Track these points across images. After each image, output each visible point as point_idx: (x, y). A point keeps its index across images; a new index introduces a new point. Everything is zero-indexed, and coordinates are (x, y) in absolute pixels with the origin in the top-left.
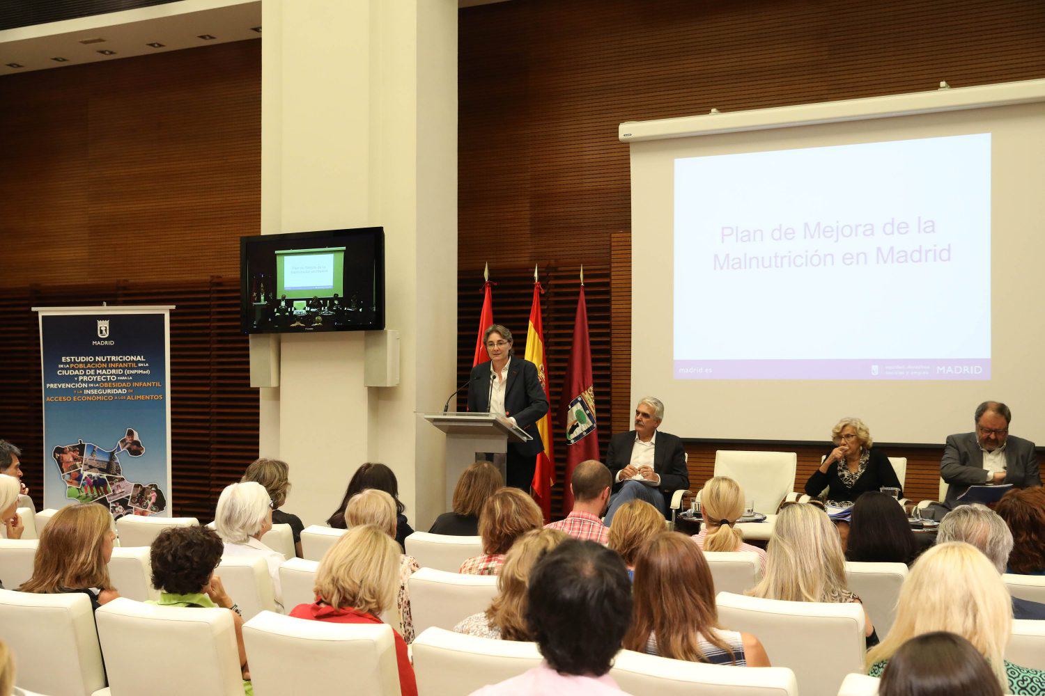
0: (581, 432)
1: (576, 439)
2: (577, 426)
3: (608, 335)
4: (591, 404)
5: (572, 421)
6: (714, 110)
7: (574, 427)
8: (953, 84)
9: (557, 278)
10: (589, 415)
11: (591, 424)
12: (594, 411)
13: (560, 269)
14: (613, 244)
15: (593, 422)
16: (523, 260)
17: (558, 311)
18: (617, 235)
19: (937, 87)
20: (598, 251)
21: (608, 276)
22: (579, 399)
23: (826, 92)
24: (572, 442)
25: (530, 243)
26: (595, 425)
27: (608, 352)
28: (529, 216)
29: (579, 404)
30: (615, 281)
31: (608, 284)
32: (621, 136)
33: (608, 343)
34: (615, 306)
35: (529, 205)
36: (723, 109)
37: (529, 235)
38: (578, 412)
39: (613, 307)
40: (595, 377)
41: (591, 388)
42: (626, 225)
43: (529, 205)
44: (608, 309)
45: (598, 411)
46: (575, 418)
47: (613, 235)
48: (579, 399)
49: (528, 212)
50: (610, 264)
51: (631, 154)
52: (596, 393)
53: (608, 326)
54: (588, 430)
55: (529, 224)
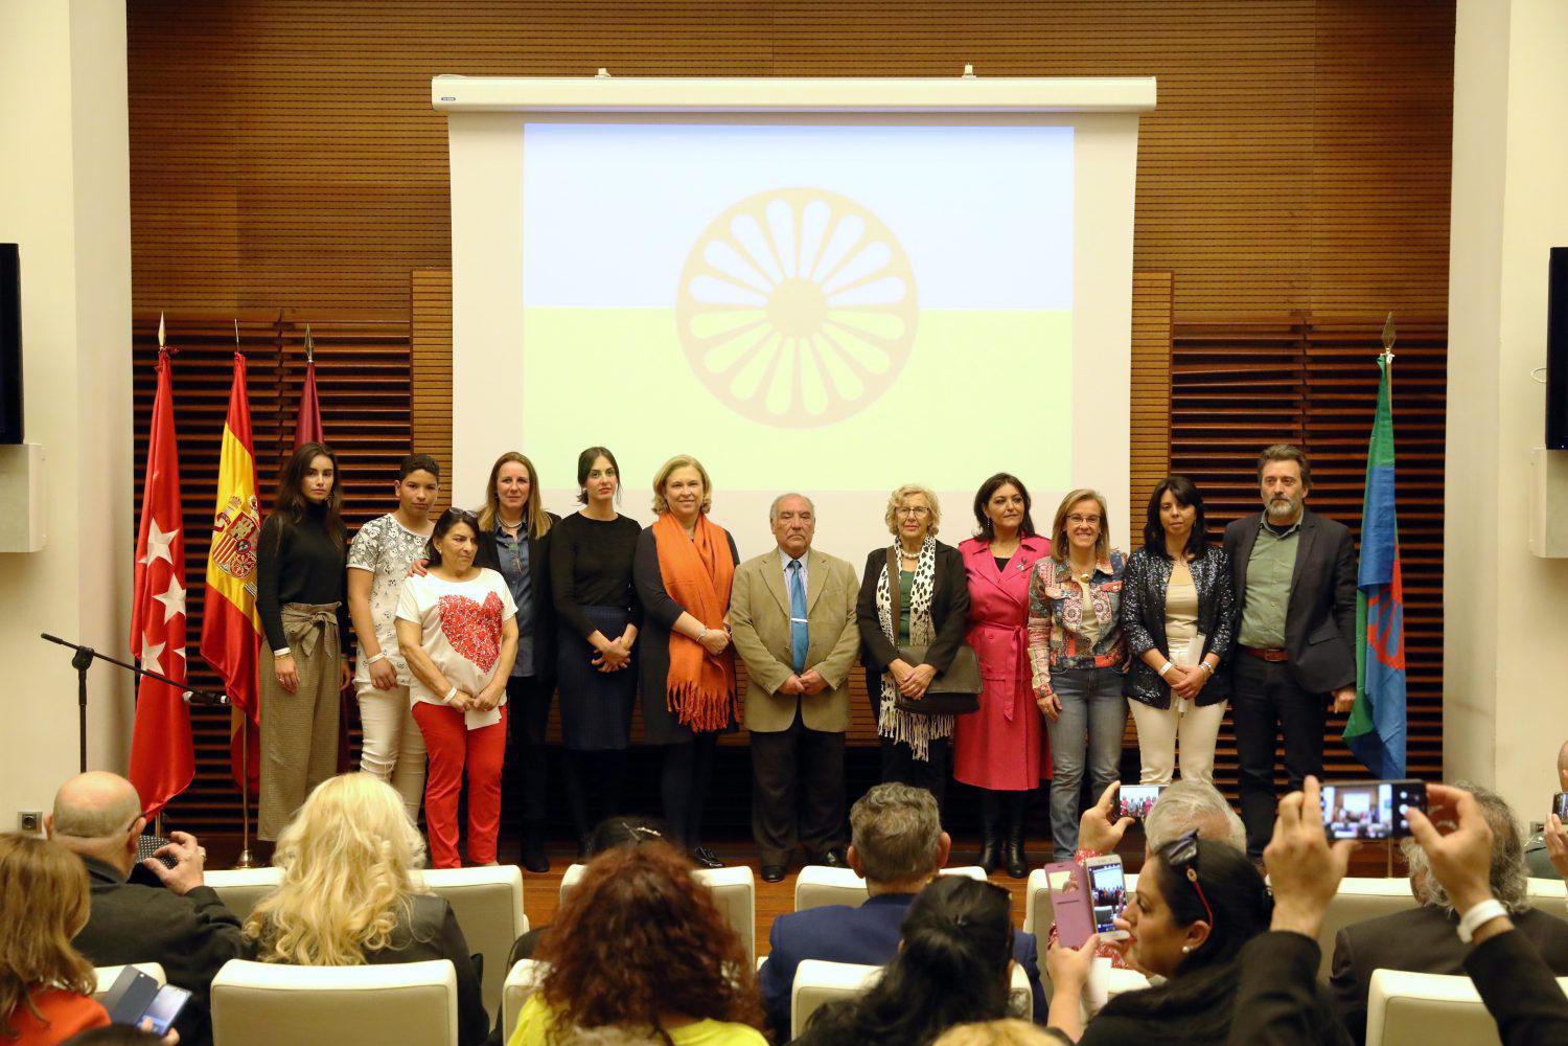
8: (978, 73)
18: (426, 274)
19: (959, 73)
20: (373, 297)
21: (406, 342)
23: (770, 57)
28: (235, 225)
30: (421, 354)
31: (406, 357)
32: (436, 99)
34: (421, 399)
37: (236, 261)
39: (416, 399)
42: (440, 255)
43: (235, 205)
44: (406, 402)
49: (235, 218)
50: (411, 323)
51: (451, 136)
55: (236, 240)
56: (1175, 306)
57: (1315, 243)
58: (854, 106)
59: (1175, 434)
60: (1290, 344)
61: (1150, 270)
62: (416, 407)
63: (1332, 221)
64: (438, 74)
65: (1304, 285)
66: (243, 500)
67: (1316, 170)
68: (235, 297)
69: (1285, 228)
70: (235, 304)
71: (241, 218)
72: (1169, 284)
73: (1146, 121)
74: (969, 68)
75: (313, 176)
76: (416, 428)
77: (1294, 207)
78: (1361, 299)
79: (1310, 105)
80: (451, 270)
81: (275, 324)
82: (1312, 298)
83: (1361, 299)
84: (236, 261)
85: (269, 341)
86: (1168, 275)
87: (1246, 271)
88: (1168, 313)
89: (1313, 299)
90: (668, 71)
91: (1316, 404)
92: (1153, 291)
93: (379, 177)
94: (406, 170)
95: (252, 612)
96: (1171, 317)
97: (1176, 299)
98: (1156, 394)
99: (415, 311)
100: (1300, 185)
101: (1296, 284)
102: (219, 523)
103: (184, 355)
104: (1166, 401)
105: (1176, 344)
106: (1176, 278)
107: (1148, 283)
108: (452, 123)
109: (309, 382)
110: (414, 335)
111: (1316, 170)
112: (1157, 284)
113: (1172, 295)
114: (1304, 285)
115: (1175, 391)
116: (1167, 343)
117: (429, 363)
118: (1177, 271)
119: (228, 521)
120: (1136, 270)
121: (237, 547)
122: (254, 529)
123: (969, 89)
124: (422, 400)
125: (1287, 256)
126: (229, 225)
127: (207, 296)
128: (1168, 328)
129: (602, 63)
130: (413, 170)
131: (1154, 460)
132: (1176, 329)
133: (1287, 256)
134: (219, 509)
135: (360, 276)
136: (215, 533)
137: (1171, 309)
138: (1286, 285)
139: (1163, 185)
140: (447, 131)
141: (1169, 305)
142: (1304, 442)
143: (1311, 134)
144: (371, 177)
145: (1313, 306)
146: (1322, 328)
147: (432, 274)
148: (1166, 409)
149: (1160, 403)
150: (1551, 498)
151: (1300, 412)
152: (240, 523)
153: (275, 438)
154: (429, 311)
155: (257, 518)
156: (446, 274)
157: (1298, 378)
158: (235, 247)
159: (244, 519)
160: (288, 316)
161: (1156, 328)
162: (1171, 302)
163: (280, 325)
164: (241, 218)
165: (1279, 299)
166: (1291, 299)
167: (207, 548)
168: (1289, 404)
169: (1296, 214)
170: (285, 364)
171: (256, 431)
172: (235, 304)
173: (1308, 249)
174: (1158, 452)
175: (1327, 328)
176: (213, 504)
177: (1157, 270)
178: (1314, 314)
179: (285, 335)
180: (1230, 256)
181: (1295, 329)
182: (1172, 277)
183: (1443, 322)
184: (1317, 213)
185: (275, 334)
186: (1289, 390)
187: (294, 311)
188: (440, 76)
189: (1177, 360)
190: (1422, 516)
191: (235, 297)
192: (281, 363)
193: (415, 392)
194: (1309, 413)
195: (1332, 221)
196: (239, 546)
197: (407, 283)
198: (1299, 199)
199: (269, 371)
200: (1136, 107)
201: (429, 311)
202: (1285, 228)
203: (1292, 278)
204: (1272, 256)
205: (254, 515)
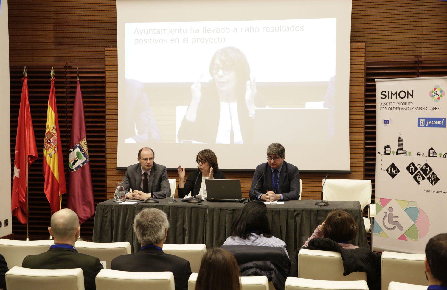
0: (80, 164)
1: (76, 168)
2: (77, 160)
4: (85, 148)
5: (74, 158)
7: (75, 162)
10: (84, 154)
11: (85, 159)
12: (87, 152)
15: (87, 158)
16: (49, 60)
22: (78, 145)
24: (75, 170)
26: (88, 160)
35: (52, 27)
37: (53, 46)
38: (78, 154)
40: (87, 132)
41: (85, 139)
43: (52, 27)
45: (89, 151)
46: (76, 156)
48: (78, 145)
49: (53, 32)
52: (88, 141)
54: (83, 163)
56: (367, 55)
60: (414, 68)
65: (419, 46)
68: (53, 58)
69: (412, 26)
70: (53, 60)
71: (55, 32)
75: (78, 17)
82: (423, 51)
84: (53, 46)
85: (63, 72)
86: (364, 44)
88: (364, 58)
92: (359, 50)
94: (107, 14)
96: (365, 59)
97: (367, 53)
98: (360, 87)
101: (417, 46)
105: (367, 69)
107: (356, 47)
110: (106, 70)
111: (425, 4)
112: (360, 47)
113: (365, 51)
114: (419, 46)
115: (367, 86)
116: (364, 68)
118: (367, 43)
120: (351, 42)
124: (109, 91)
128: (364, 63)
132: (367, 63)
135: (93, 50)
137: (365, 57)
139: (367, 12)
141: (364, 55)
144: (96, 17)
145: (423, 54)
147: (111, 49)
148: (363, 92)
153: (64, 105)
158: (53, 41)
160: (69, 64)
161: (360, 63)
162: (365, 54)
163: (66, 67)
164: (55, 32)
165: (410, 52)
166: (416, 52)
169: (417, 20)
170: (68, 80)
172: (53, 60)
173: (421, 33)
174: (360, 108)
178: (423, 57)
179: (68, 70)
180: (392, 37)
181: (416, 62)
182: (365, 46)
185: (64, 70)
191: (53, 58)
198: (418, 15)
199: (63, 82)
201: (111, 62)
202: (412, 26)
203: (415, 44)
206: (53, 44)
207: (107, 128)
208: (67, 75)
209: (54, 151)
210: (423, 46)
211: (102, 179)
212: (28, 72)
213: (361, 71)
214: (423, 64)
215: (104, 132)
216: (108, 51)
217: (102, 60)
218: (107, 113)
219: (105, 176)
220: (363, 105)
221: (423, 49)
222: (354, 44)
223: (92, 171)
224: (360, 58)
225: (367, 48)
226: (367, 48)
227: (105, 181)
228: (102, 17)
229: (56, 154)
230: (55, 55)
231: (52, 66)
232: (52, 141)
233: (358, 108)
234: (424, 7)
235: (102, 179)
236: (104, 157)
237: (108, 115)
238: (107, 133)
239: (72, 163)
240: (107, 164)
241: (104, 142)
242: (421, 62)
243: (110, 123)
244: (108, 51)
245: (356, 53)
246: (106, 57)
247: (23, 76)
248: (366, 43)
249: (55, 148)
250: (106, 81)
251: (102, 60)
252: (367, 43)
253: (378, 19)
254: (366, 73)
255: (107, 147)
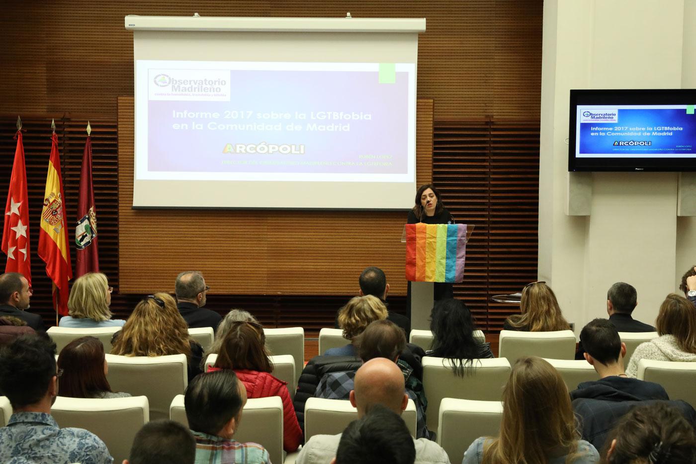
3: (116, 170)
6: (196, 14)
8: (353, 16)
9: (70, 126)
13: (73, 120)
14: (119, 104)
16: (41, 111)
17: (71, 151)
18: (123, 98)
19: (345, 16)
21: (116, 127)
25: (47, 98)
27: (116, 183)
28: (45, 77)
29: (86, 220)
30: (122, 131)
31: (115, 133)
32: (127, 25)
33: (116, 176)
36: (202, 14)
39: (119, 150)
44: (116, 152)
47: (119, 98)
49: (45, 74)
53: (116, 164)
57: (495, 87)
58: (263, 29)
59: (435, 167)
60: (485, 130)
61: (424, 98)
62: (119, 154)
63: (502, 78)
64: (127, 15)
66: (56, 194)
67: (496, 57)
69: (483, 81)
72: (432, 104)
73: (421, 36)
74: (349, 14)
75: (78, 57)
76: (120, 162)
77: (487, 72)
78: (514, 111)
79: (493, 30)
80: (134, 97)
81: (62, 119)
83: (514, 111)
84: (45, 93)
86: (432, 101)
87: (467, 99)
88: (432, 116)
89: (494, 111)
90: (232, 14)
91: (495, 154)
92: (426, 107)
93: (107, 57)
95: (57, 239)
97: (435, 111)
99: (119, 114)
100: (489, 63)
101: (487, 105)
102: (45, 203)
103: (28, 132)
104: (431, 153)
105: (435, 129)
106: (435, 102)
107: (423, 104)
108: (135, 36)
109: (88, 143)
111: (496, 57)
113: (433, 108)
114: (491, 105)
115: (435, 149)
116: (431, 128)
117: (125, 135)
118: (436, 99)
119: (49, 202)
120: (418, 98)
121: (52, 213)
122: (59, 206)
123: (349, 23)
125: (484, 93)
126: (43, 77)
127: (35, 107)
128: (432, 122)
129: (195, 11)
130: (120, 55)
131: (426, 177)
132: (435, 123)
133: (484, 93)
134: (46, 197)
136: (44, 207)
137: (433, 115)
138: (484, 105)
140: (133, 38)
141: (432, 113)
142: (490, 170)
143: (494, 42)
144: (102, 57)
145: (494, 114)
146: (499, 123)
147: (126, 98)
148: (431, 156)
149: (429, 154)
150: (571, 191)
151: (488, 158)
152: (54, 203)
154: (125, 114)
155: (61, 202)
156: (131, 98)
157: (487, 144)
159: (56, 202)
160: (67, 115)
161: (427, 122)
167: (40, 212)
168: (484, 155)
169: (488, 75)
171: (61, 163)
172: (45, 110)
173: (493, 90)
175: (502, 123)
176: (43, 194)
177: (429, 98)
178: (494, 117)
180: (460, 93)
181: (487, 123)
183: (538, 121)
184: (496, 75)
185: (62, 123)
186: (484, 148)
187: (70, 114)
188: (129, 16)
189: (435, 136)
190: (530, 201)
192: (64, 135)
193: (119, 147)
194: (492, 158)
195: (502, 78)
196: (54, 212)
197: (115, 102)
200: (418, 30)
201: (125, 114)
203: (486, 102)
204: (478, 93)
205: (60, 200)
206: (46, 89)
207: (120, 196)
208: (65, 130)
209: (61, 225)
210: (495, 105)
211: (114, 259)
212: (24, 125)
213: (429, 132)
214: (495, 125)
215: (117, 201)
216: (121, 101)
217: (114, 111)
218: (120, 178)
219: (117, 256)
220: (431, 171)
221: (494, 108)
222: (421, 100)
223: (99, 250)
224: (428, 116)
225: (435, 105)
226: (435, 105)
227: (117, 262)
228: (110, 57)
229: (63, 228)
230: (48, 104)
231: (52, 118)
232: (59, 213)
233: (426, 174)
234: (496, 60)
235: (114, 259)
236: (117, 232)
237: (122, 180)
238: (120, 202)
239: (79, 239)
240: (120, 241)
241: (117, 213)
242: (493, 123)
243: (124, 190)
244: (121, 101)
245: (423, 110)
246: (119, 108)
247: (16, 131)
248: (434, 99)
249: (62, 220)
250: (119, 138)
251: (114, 111)
252: (436, 99)
253: (445, 72)
254: (434, 134)
255: (120, 220)
